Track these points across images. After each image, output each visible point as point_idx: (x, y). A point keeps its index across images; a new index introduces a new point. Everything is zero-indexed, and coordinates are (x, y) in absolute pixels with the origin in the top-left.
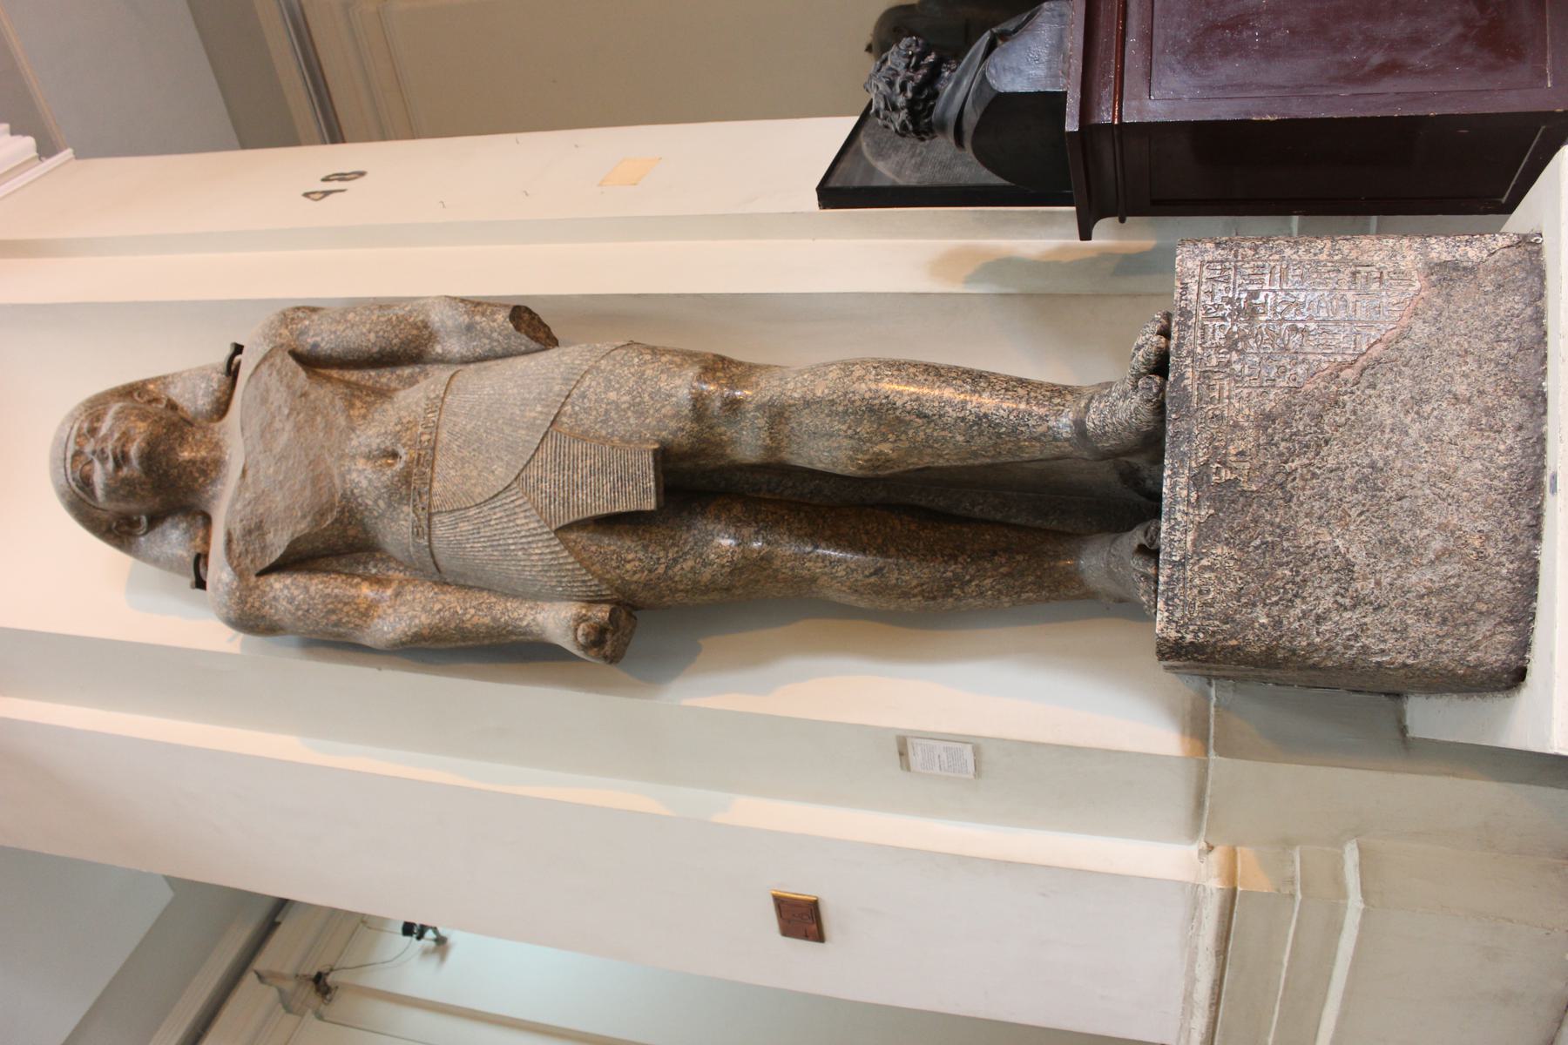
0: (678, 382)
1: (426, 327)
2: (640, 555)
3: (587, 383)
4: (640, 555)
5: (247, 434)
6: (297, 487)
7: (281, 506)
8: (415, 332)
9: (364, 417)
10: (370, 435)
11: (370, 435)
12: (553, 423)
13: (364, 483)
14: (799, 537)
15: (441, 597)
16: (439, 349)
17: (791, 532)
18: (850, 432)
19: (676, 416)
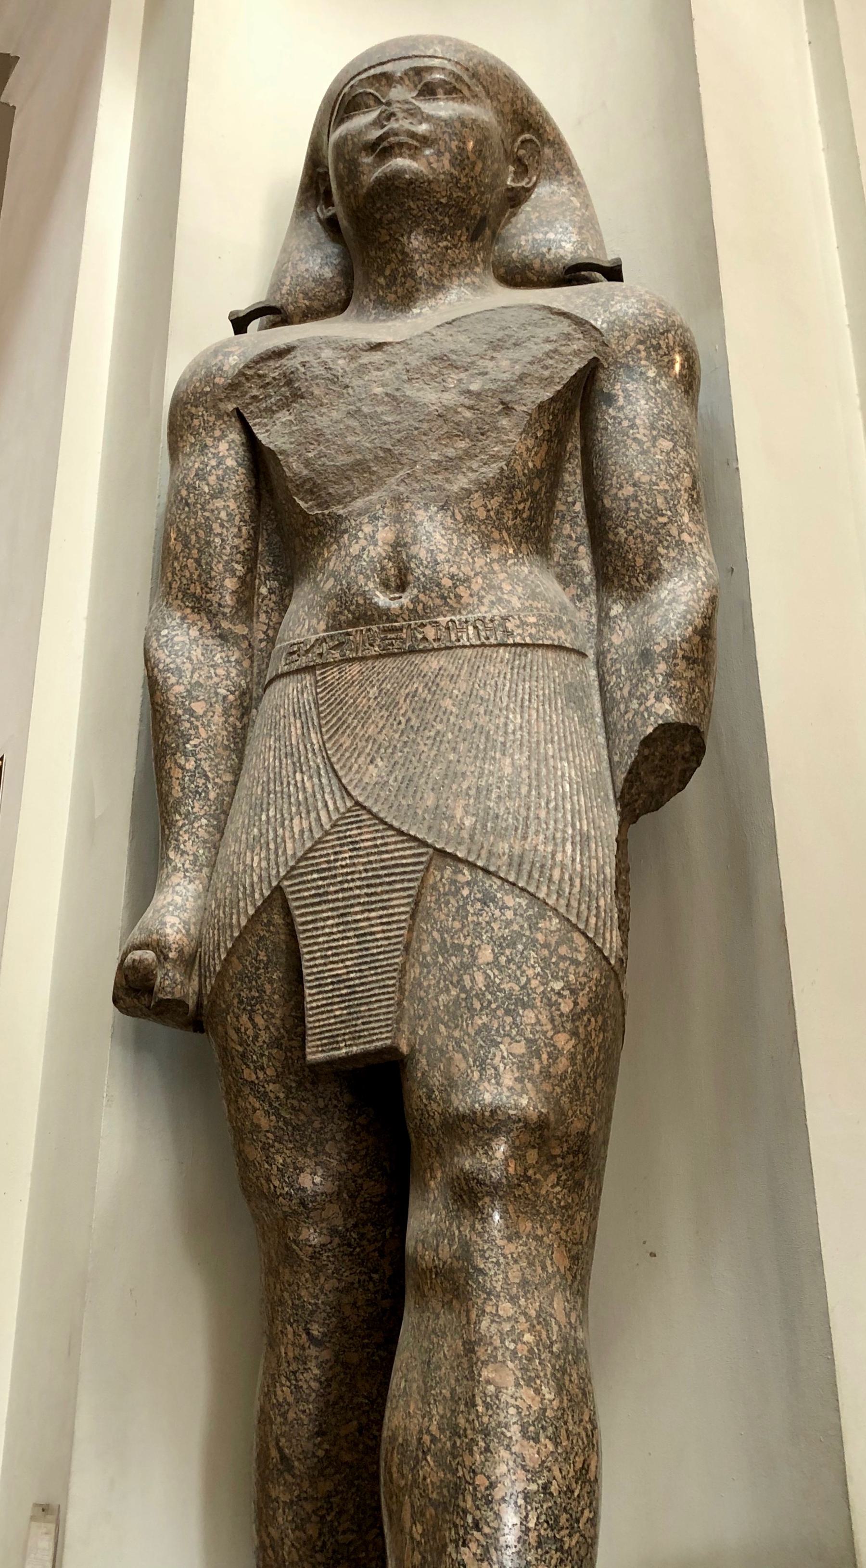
0: (508, 1080)
1: (650, 579)
2: (264, 1036)
3: (510, 901)
4: (264, 1036)
5: (440, 334)
6: (351, 439)
7: (322, 422)
8: (640, 561)
9: (469, 519)
10: (435, 538)
11: (435, 538)
12: (442, 853)
13: (355, 549)
14: (337, 1308)
15: (219, 708)
16: (616, 609)
17: (347, 1290)
18: (427, 1438)
19: (451, 1083)
